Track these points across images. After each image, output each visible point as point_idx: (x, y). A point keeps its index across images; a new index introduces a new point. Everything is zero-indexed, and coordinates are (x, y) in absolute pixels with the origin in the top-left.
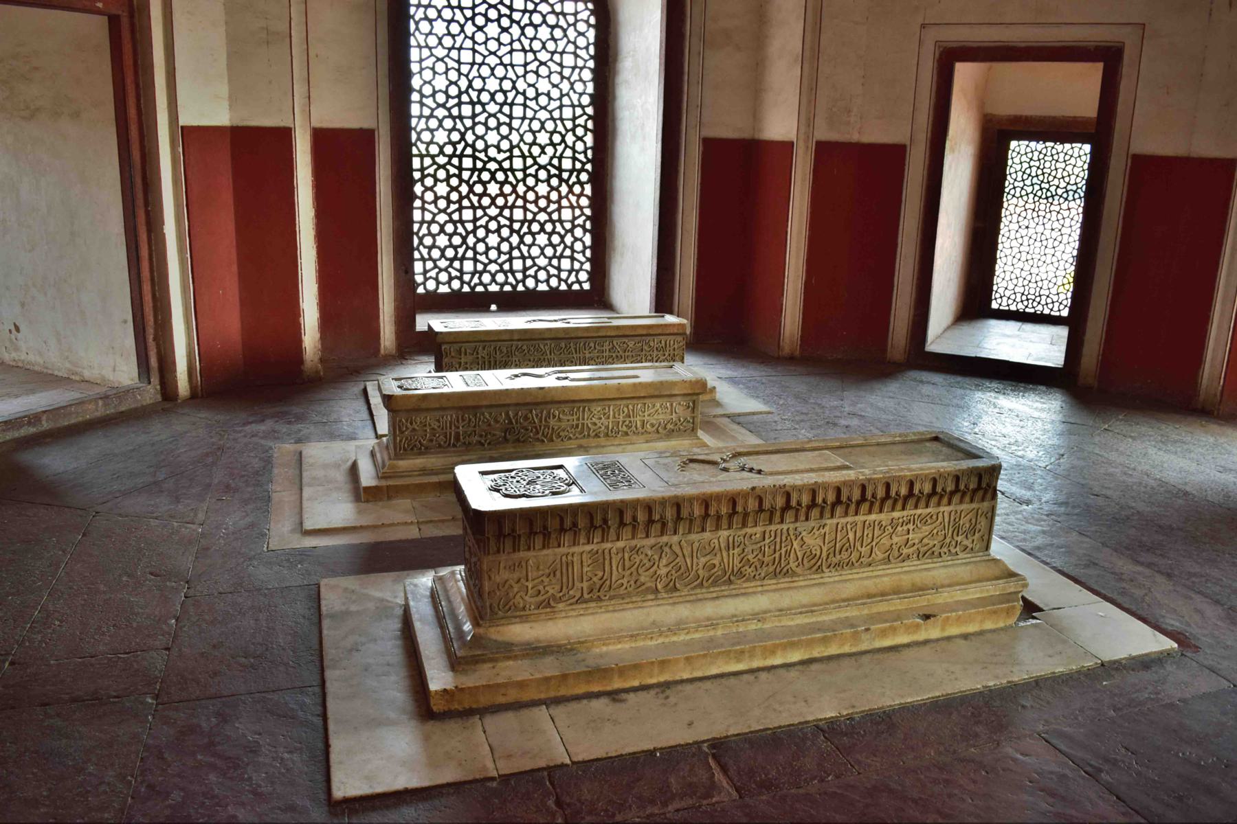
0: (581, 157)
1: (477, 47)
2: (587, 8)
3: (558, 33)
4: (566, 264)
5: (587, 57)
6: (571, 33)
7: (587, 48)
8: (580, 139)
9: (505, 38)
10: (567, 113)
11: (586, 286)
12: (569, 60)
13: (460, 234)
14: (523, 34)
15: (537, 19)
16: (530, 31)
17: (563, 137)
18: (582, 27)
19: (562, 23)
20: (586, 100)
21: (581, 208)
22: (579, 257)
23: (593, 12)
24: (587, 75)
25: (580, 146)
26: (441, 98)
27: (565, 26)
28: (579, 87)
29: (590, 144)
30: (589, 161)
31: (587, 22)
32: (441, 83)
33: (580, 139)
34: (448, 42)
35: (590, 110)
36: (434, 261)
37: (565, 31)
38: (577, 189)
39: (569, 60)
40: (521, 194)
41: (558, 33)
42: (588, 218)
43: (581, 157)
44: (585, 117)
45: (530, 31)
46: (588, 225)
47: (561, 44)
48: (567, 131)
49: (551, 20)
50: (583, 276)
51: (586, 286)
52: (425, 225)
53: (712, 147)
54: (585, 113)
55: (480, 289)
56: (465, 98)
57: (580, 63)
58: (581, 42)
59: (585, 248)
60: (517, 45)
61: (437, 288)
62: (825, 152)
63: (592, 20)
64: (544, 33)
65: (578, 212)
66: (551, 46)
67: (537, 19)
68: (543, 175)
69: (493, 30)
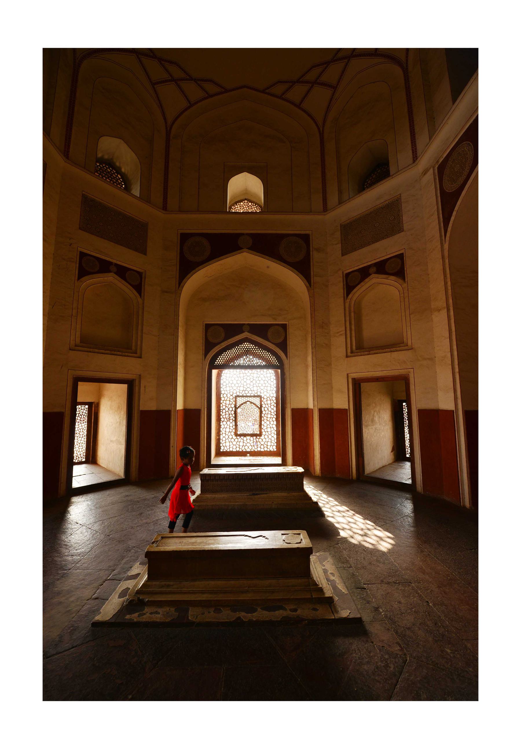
3: (266, 382)
4: (269, 444)
11: (275, 450)
12: (269, 388)
15: (260, 379)
16: (258, 382)
19: (266, 379)
22: (273, 442)
24: (274, 392)
38: (272, 423)
39: (269, 388)
45: (258, 382)
50: (275, 447)
51: (275, 450)
53: (293, 410)
55: (244, 450)
57: (272, 389)
58: (272, 384)
62: (322, 412)
63: (275, 378)
67: (260, 379)
69: (248, 382)
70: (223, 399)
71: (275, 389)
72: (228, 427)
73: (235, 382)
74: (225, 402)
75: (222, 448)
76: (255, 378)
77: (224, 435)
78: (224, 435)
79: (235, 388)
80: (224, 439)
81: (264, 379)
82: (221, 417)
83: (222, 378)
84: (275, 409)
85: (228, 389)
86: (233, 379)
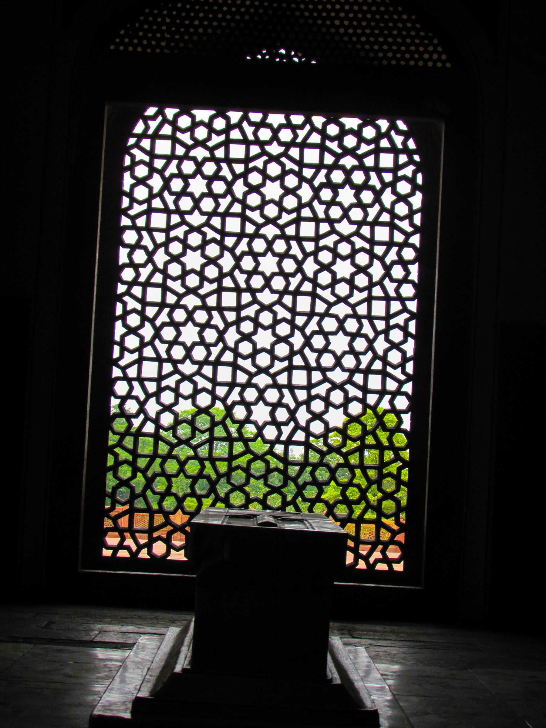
0: (398, 373)
1: (248, 213)
2: (411, 161)
3: (367, 197)
5: (410, 229)
6: (388, 198)
7: (410, 217)
8: (394, 346)
9: (290, 202)
10: (379, 308)
11: (399, 567)
13: (208, 478)
14: (316, 196)
15: (338, 177)
16: (326, 194)
17: (371, 343)
18: (404, 188)
19: (374, 181)
20: (408, 290)
21: (396, 451)
23: (419, 168)
25: (395, 357)
26: (192, 281)
27: (378, 186)
28: (398, 272)
29: (410, 353)
30: (409, 378)
31: (412, 181)
32: (193, 260)
33: (394, 346)
34: (208, 205)
35: (412, 306)
36: (166, 515)
37: (378, 195)
40: (303, 423)
41: (367, 197)
42: (405, 464)
43: (398, 373)
44: (406, 315)
46: (405, 475)
47: (373, 212)
48: (377, 333)
49: (358, 177)
50: (393, 553)
52: (158, 461)
54: (405, 309)
56: (227, 282)
57: (399, 237)
58: (401, 209)
59: (399, 509)
60: (306, 212)
61: (168, 553)
63: (419, 179)
64: (346, 196)
65: (389, 455)
66: (356, 214)
68: (337, 397)
70: (128, 274)
71: (416, 240)
72: (150, 428)
73: (198, 186)
74: (137, 291)
75: (112, 540)
76: (308, 173)
77: (125, 472)
78: (125, 472)
79: (196, 219)
80: (124, 493)
81: (358, 177)
82: (116, 372)
83: (127, 161)
84: (410, 347)
85: (159, 220)
86: (188, 167)
